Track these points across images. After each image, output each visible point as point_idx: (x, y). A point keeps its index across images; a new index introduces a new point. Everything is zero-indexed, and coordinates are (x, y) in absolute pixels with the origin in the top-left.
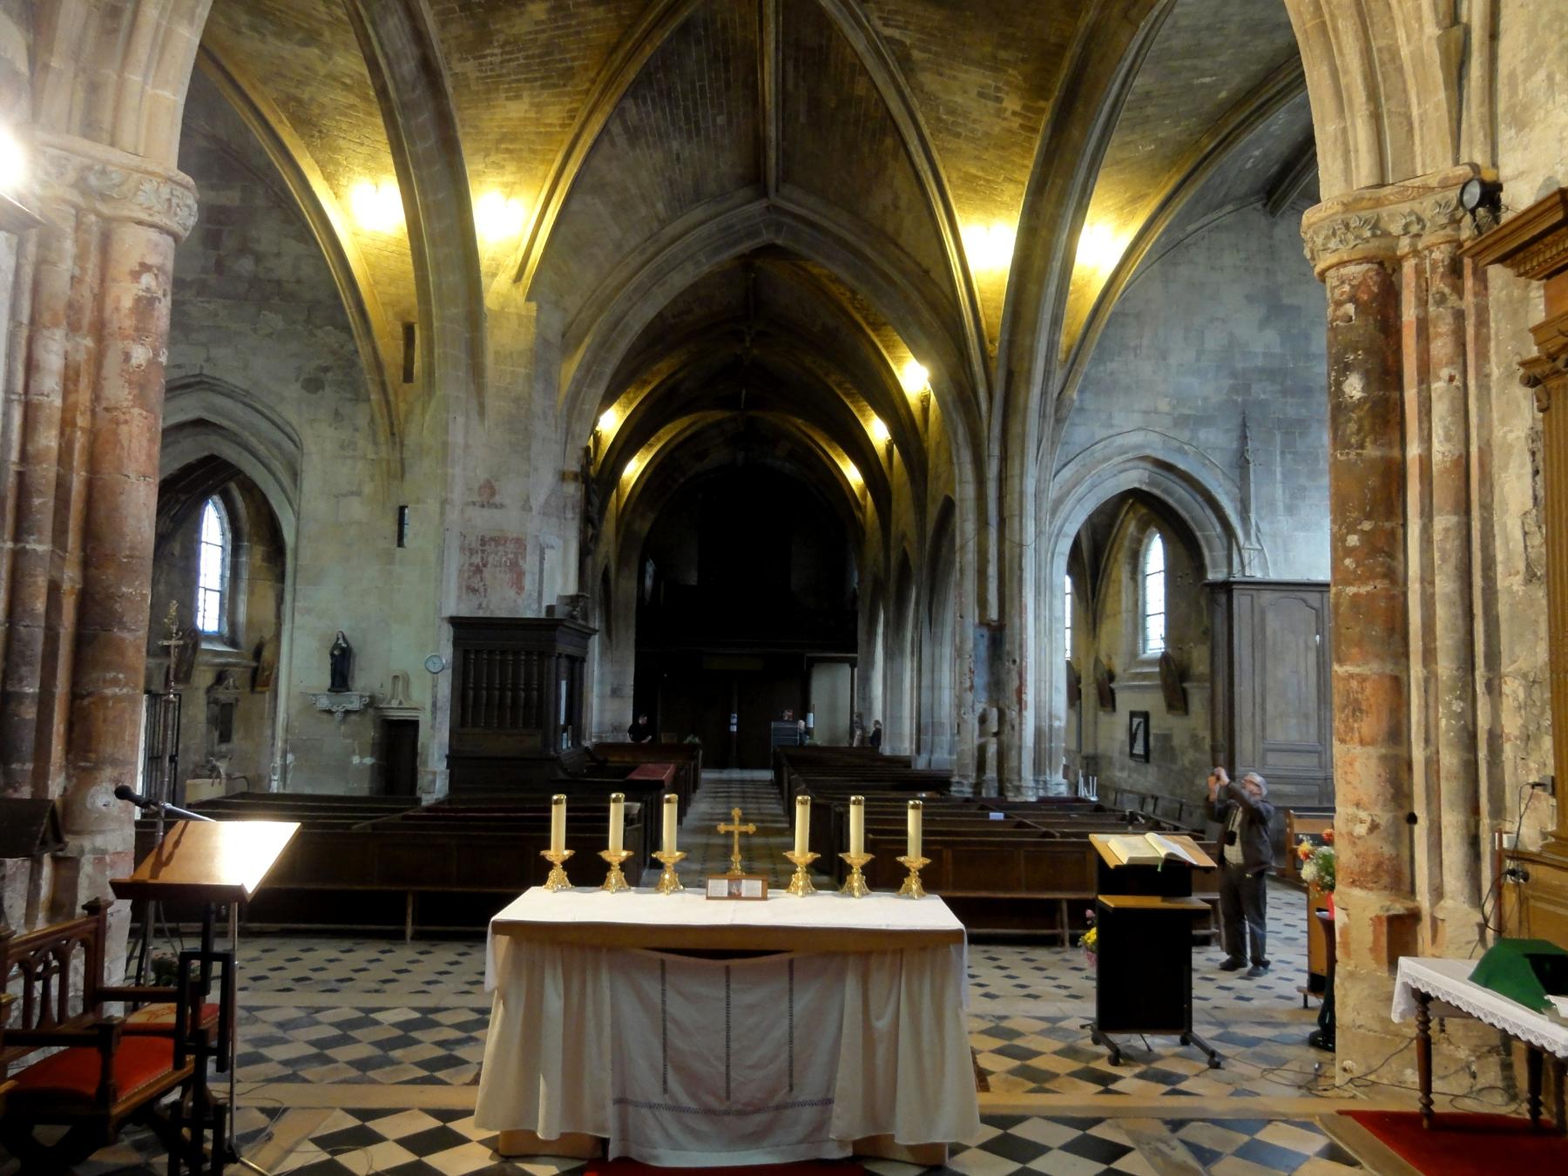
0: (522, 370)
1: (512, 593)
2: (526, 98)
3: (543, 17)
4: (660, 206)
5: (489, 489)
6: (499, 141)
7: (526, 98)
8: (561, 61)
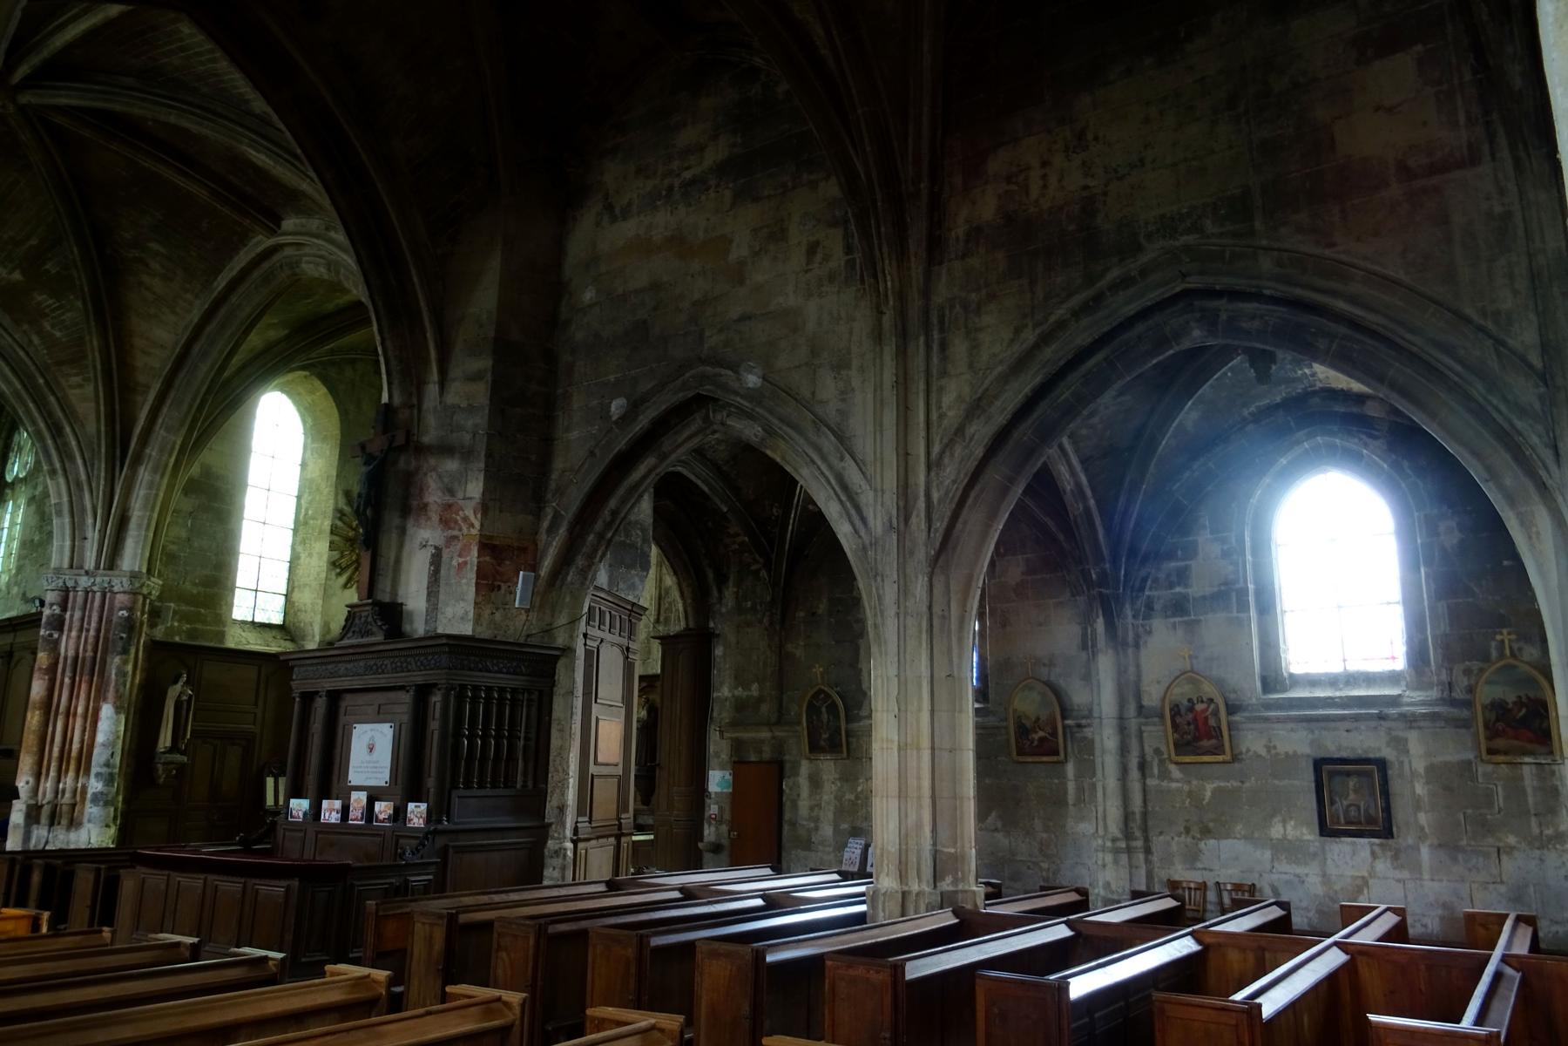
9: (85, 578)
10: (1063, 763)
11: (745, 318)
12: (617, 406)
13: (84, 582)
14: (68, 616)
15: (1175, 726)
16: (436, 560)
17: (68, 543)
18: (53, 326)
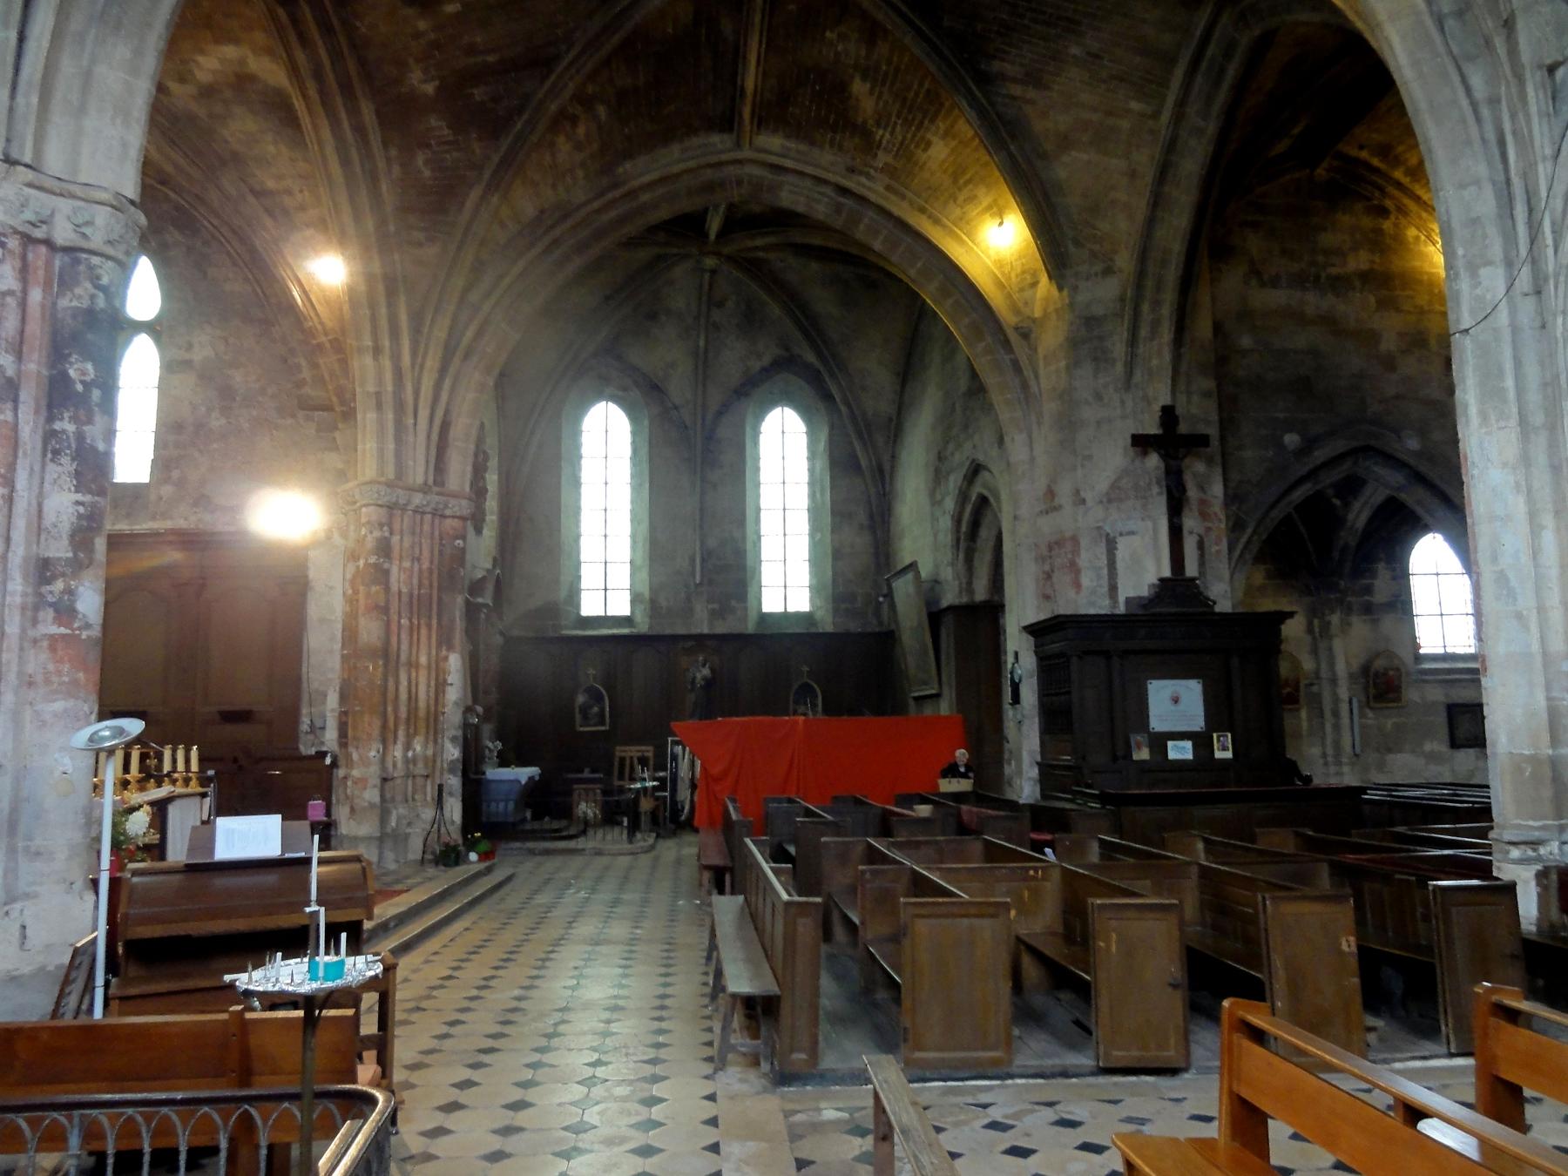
0: (1063, 363)
1: (1072, 593)
2: (935, 139)
3: (868, 85)
4: (1135, 105)
5: (1051, 493)
6: (955, 181)
7: (935, 139)
8: (917, 94)
9: (420, 495)
10: (1298, 710)
11: (1397, 397)
12: (1291, 440)
13: (418, 499)
14: (396, 539)
15: (1375, 684)
16: (1201, 545)
17: (391, 446)
18: (426, 162)
